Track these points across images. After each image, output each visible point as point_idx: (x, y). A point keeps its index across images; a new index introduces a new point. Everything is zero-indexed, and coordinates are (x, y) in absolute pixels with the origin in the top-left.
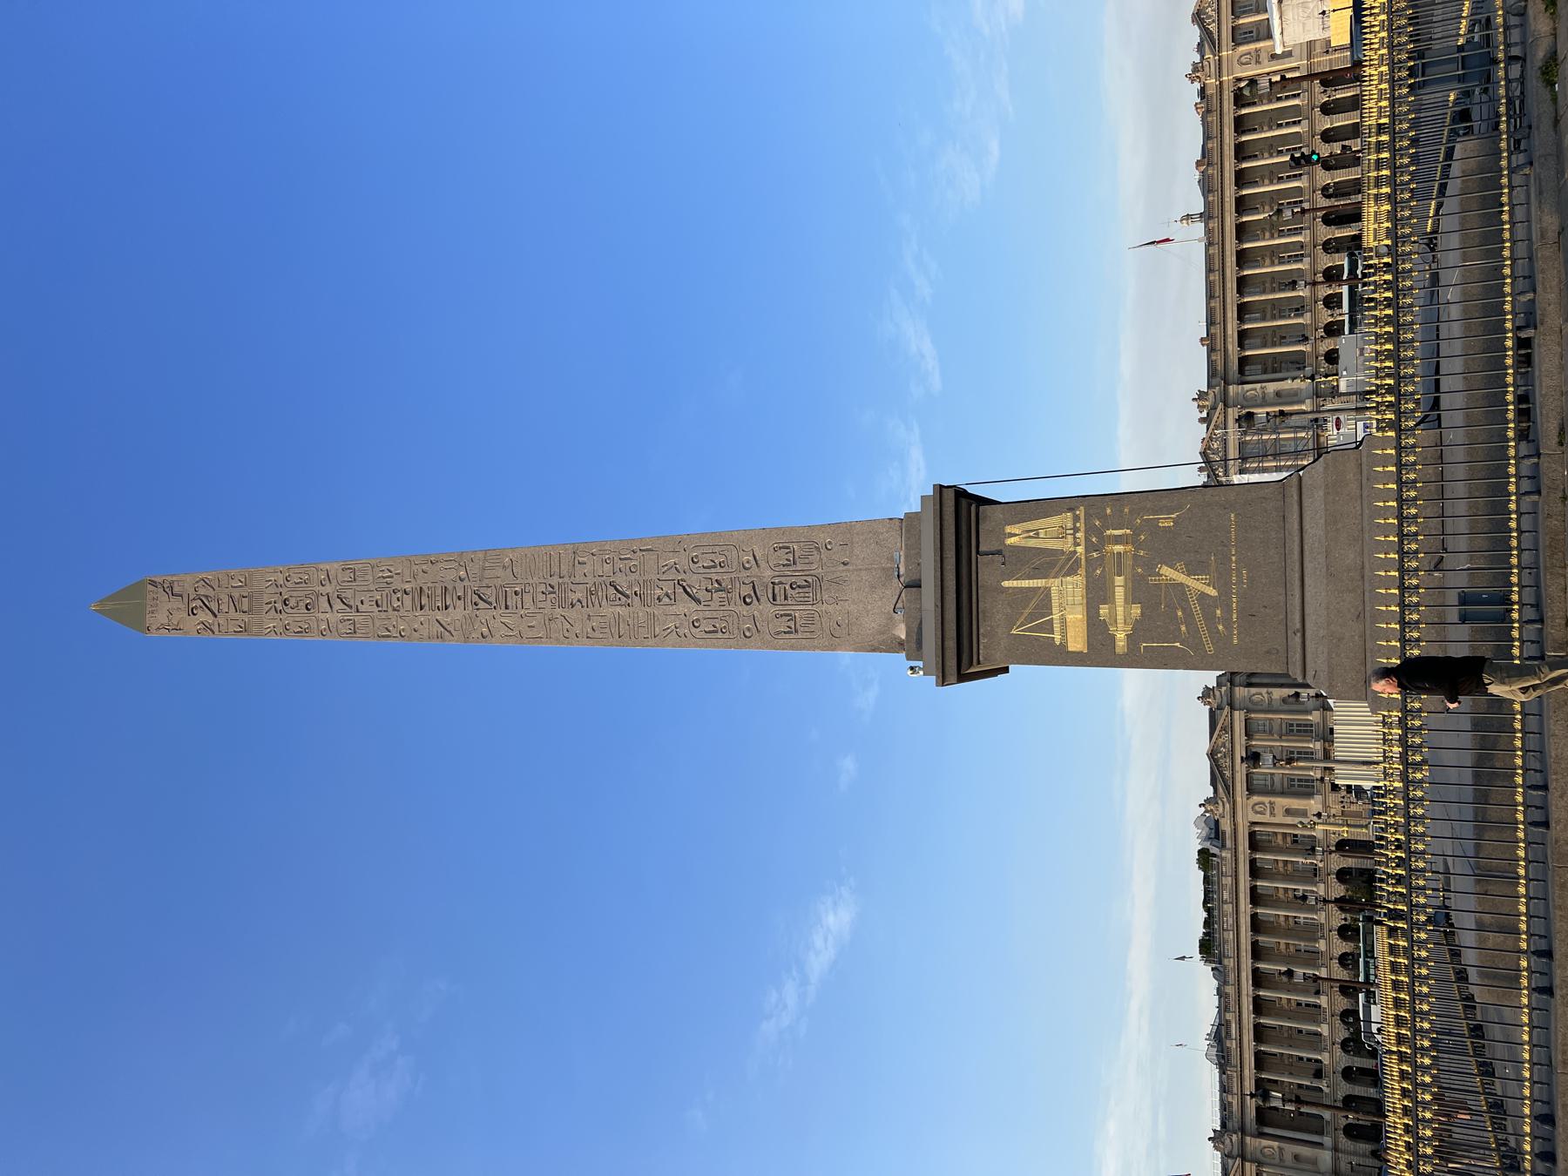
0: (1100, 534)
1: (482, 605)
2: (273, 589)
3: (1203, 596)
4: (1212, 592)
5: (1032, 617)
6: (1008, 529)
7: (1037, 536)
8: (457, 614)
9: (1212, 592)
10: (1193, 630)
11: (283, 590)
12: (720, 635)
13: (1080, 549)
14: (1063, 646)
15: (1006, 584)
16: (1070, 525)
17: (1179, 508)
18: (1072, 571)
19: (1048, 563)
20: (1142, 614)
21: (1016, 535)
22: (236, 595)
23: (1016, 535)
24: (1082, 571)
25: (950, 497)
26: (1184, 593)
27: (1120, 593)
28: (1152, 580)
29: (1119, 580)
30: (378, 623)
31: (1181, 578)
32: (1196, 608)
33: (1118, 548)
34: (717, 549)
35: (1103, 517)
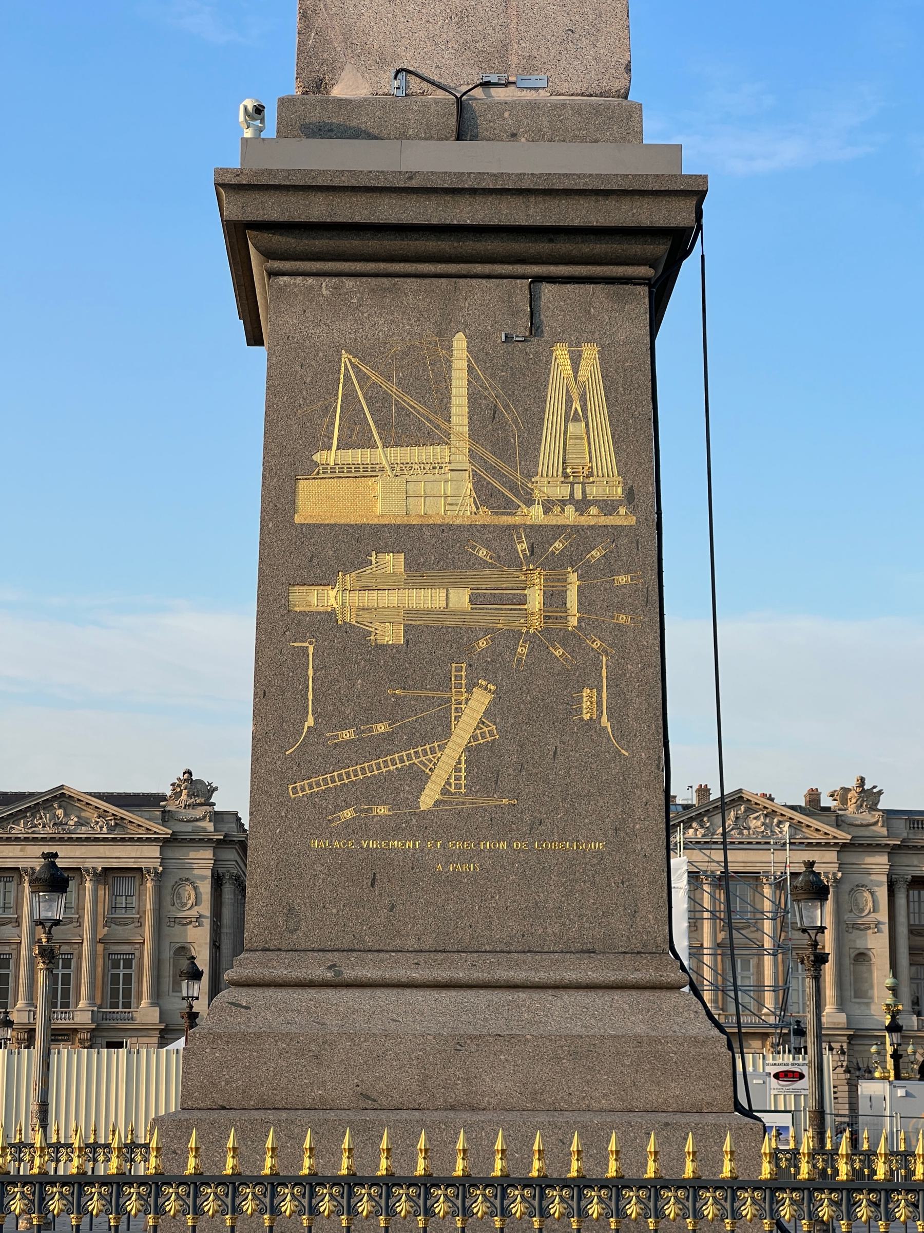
0: (570, 559)
3: (419, 778)
4: (428, 799)
6: (590, 353)
7: (570, 417)
9: (428, 799)
10: (341, 756)
13: (536, 515)
14: (312, 470)
15: (460, 343)
16: (594, 492)
18: (485, 494)
19: (506, 437)
21: (573, 370)
24: (485, 517)
25: (675, 215)
26: (426, 738)
27: (430, 599)
28: (460, 671)
29: (460, 598)
31: (464, 731)
32: (391, 763)
33: (535, 599)
35: (609, 567)
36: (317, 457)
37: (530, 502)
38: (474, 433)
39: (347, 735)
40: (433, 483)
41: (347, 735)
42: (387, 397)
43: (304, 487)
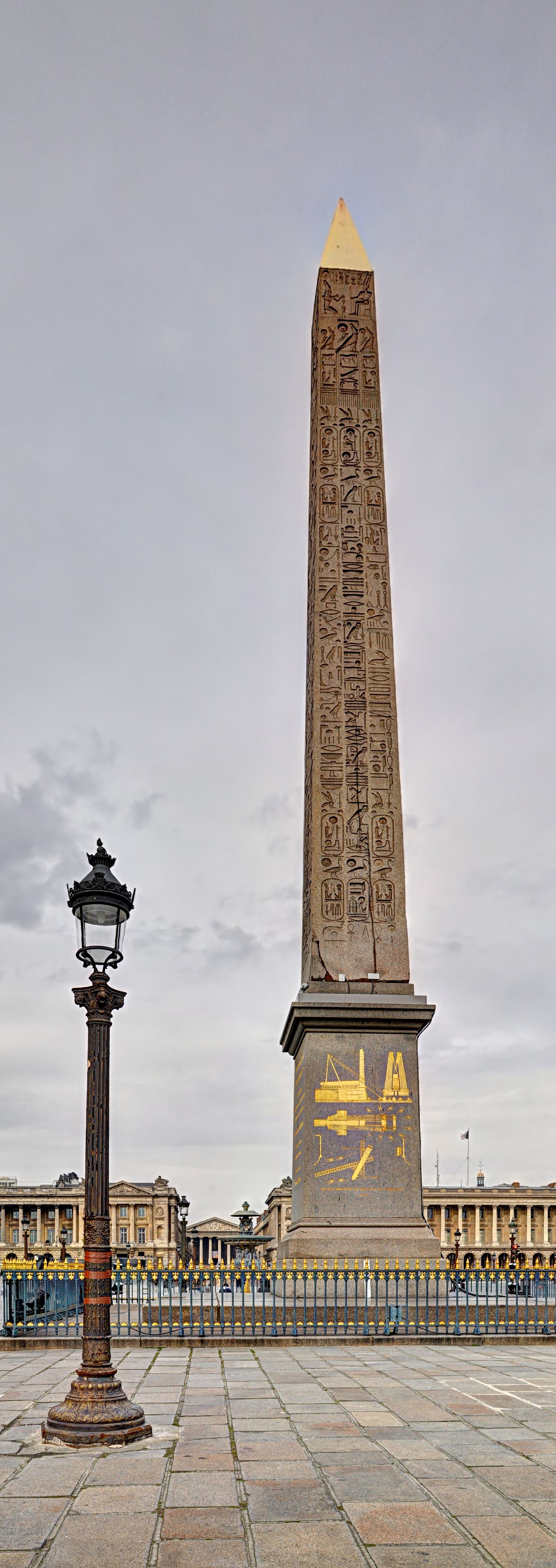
1: (348, 629)
2: (363, 417)
3: (352, 1172)
4: (354, 1177)
5: (338, 1068)
6: (399, 1055)
7: (394, 1072)
8: (341, 604)
9: (354, 1177)
10: (329, 1166)
11: (361, 429)
12: (324, 839)
13: (384, 1100)
14: (320, 1087)
15: (362, 1052)
16: (400, 1094)
17: (409, 1159)
19: (376, 1078)
20: (341, 1136)
21: (395, 1060)
22: (357, 376)
23: (395, 1060)
26: (353, 1161)
27: (354, 1123)
29: (363, 1123)
30: (333, 526)
33: (384, 1123)
34: (391, 839)
36: (322, 1084)
37: (382, 1096)
38: (366, 1079)
39: (331, 1160)
40: (354, 1091)
41: (331, 1160)
42: (341, 1067)
43: (317, 1092)
